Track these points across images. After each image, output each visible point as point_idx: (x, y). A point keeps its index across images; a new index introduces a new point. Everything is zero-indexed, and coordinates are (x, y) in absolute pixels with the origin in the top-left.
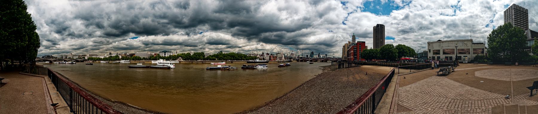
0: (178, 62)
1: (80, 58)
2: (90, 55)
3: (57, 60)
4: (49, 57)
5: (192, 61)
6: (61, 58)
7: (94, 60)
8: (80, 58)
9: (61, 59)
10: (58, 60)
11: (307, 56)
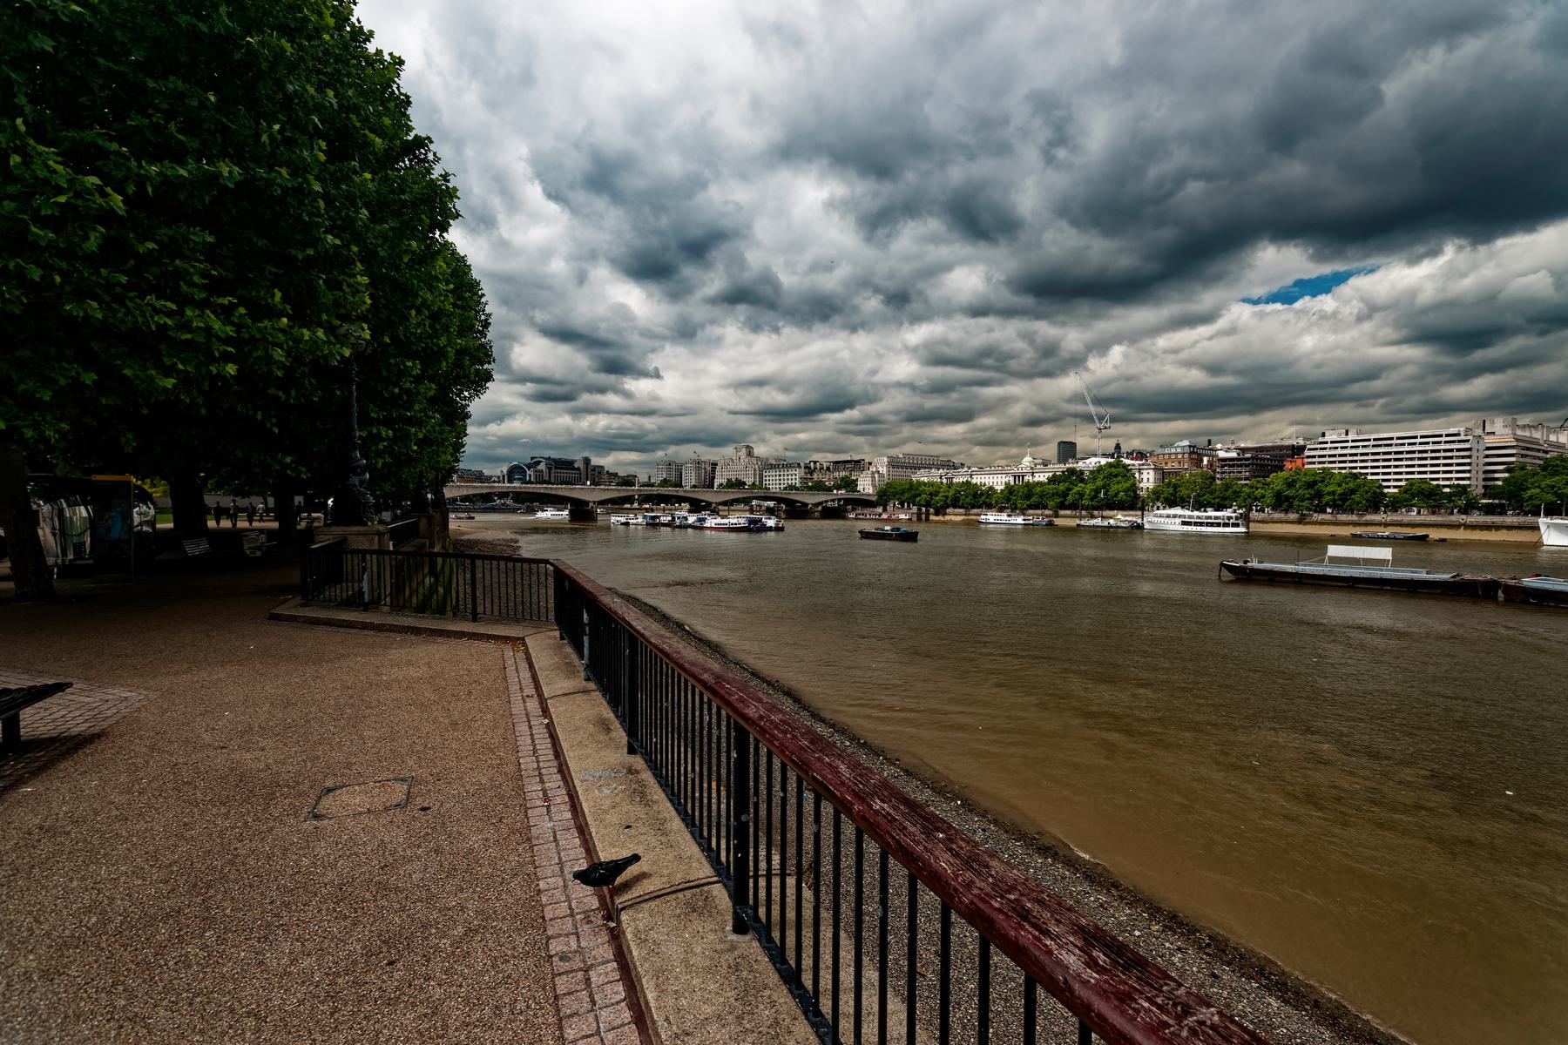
1: (819, 487)
3: (630, 499)
4: (564, 474)
6: (665, 483)
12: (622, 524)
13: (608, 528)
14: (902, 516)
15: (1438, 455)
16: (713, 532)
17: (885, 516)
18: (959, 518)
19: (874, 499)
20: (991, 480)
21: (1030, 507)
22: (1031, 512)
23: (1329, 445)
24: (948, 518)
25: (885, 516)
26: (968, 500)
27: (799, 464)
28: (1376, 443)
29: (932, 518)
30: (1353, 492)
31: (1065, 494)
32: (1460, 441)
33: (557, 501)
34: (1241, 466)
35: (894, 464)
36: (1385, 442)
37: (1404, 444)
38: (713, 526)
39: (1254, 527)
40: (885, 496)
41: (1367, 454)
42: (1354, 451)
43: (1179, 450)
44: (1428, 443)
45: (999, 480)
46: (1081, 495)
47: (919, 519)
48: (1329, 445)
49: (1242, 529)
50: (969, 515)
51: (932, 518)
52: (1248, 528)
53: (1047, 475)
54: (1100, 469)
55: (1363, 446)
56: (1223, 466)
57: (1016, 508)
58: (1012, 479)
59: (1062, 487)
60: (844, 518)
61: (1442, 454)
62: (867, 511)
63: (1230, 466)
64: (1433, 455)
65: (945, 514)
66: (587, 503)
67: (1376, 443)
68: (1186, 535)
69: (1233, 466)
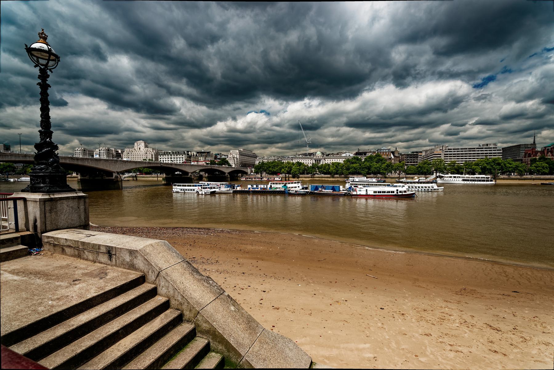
15: (467, 155)
16: (371, 202)
18: (308, 179)
20: (307, 162)
23: (460, 150)
27: (184, 152)
28: (469, 150)
32: (497, 150)
34: (414, 157)
35: (241, 154)
36: (473, 150)
37: (479, 151)
38: (372, 193)
39: (499, 182)
41: (467, 154)
42: (486, 152)
43: (387, 151)
44: (487, 150)
45: (309, 162)
48: (452, 150)
49: (493, 182)
50: (314, 177)
51: (290, 179)
52: (496, 182)
53: (343, 160)
55: (457, 151)
56: (407, 157)
57: (343, 174)
58: (314, 162)
61: (453, 155)
63: (411, 157)
64: (490, 155)
65: (298, 177)
66: (110, 173)
67: (469, 150)
68: (464, 186)
69: (411, 157)
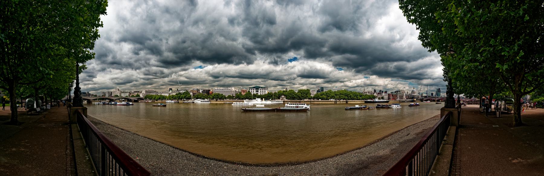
0: (283, 102)
2: (146, 92)
3: (96, 99)
4: (85, 95)
5: (299, 101)
6: (103, 96)
7: (154, 99)
8: (133, 96)
9: (103, 97)
10: (100, 99)
11: (432, 94)
12: (98, 104)
13: (94, 105)
14: (150, 101)
17: (146, 101)
19: (144, 98)
21: (173, 99)
22: (173, 100)
24: (158, 101)
25: (146, 101)
26: (162, 98)
29: (155, 101)
30: (223, 97)
31: (179, 97)
33: (85, 99)
40: (146, 97)
46: (182, 97)
47: (153, 102)
51: (155, 101)
54: (184, 93)
59: (179, 96)
60: (138, 102)
62: (143, 100)
66: (90, 100)
